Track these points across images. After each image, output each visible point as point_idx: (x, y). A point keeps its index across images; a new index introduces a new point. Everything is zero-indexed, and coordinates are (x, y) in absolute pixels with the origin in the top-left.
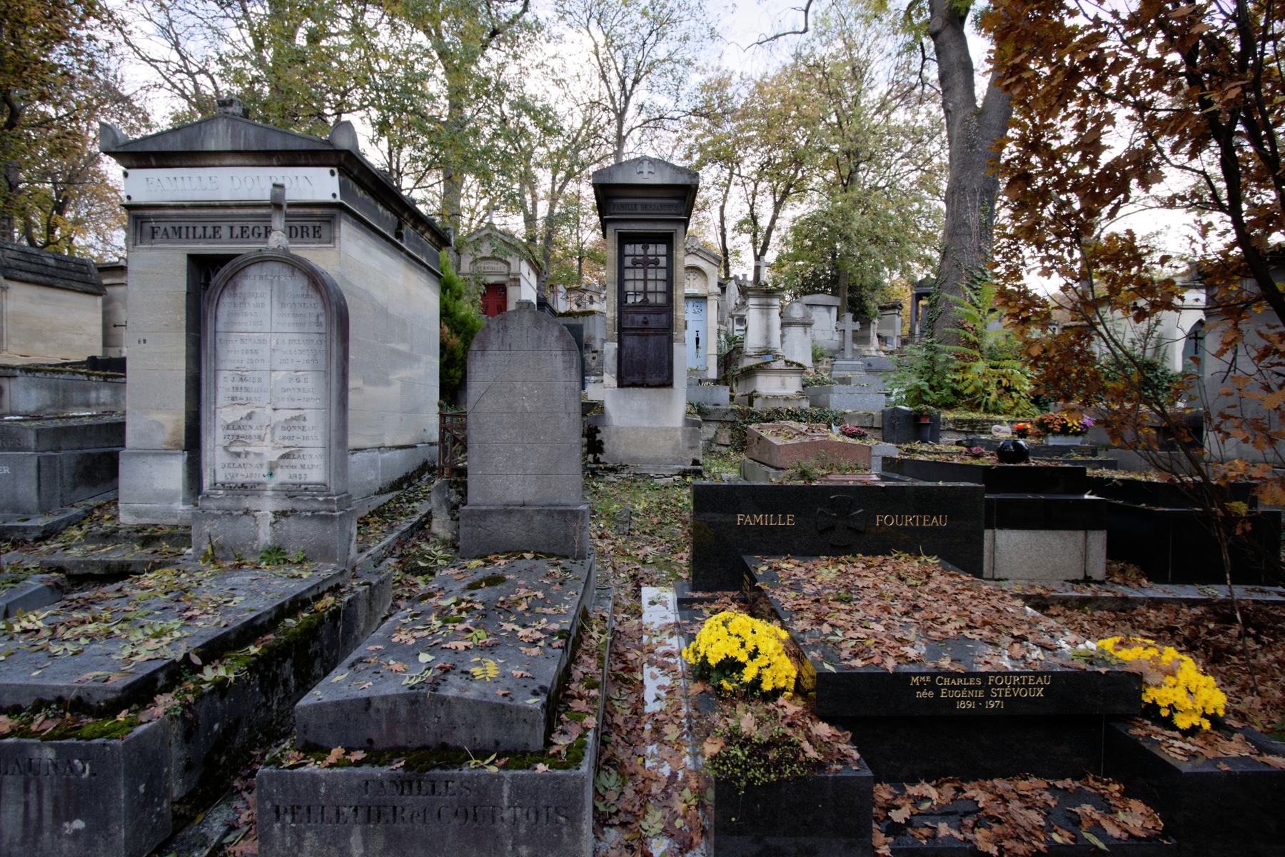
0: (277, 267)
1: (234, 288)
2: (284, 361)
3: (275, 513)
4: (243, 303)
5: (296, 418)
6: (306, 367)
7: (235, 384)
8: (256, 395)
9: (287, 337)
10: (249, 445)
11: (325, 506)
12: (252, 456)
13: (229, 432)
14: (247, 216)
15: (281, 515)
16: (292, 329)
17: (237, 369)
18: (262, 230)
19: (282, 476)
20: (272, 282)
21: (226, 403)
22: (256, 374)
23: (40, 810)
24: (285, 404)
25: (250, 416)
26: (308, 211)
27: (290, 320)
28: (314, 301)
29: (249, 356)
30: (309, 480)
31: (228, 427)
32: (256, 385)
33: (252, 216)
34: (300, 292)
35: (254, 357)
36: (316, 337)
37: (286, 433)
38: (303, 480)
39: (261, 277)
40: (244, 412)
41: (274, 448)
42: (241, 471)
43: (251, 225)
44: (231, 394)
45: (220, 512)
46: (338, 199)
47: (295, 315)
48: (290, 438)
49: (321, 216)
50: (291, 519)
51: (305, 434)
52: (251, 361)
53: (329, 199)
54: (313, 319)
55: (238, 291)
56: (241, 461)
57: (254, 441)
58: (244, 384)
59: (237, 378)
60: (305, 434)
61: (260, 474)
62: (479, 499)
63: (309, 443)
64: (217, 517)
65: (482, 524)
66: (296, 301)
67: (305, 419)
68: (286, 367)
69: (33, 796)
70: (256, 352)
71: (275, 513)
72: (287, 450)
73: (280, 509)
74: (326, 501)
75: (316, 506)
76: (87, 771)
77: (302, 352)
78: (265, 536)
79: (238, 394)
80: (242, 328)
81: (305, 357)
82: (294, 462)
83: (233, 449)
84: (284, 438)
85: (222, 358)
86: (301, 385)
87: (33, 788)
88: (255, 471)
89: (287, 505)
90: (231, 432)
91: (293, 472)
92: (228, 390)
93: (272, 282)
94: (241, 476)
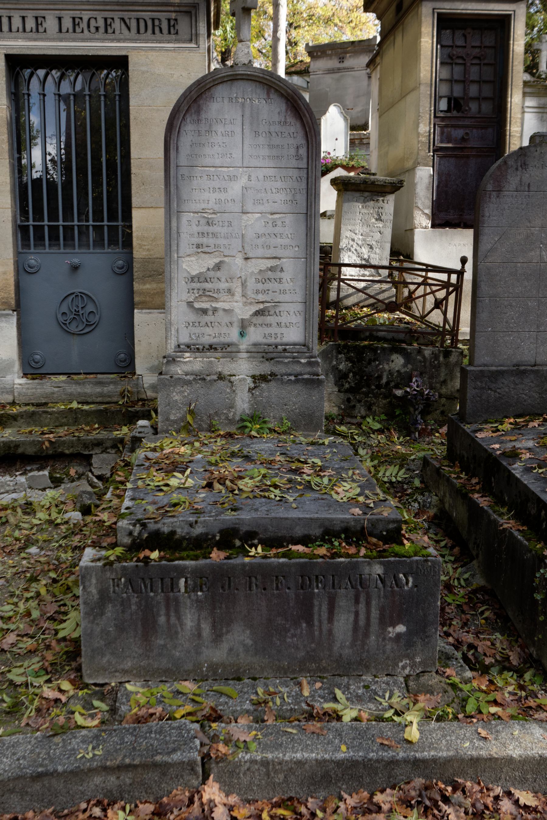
0: (249, 88)
1: (198, 112)
2: (259, 202)
3: (253, 377)
4: (209, 131)
5: (272, 269)
7: (200, 229)
8: (225, 242)
10: (216, 300)
11: (308, 369)
12: (221, 313)
13: (194, 285)
15: (260, 379)
17: (204, 211)
18: (101, 23)
19: (255, 335)
21: (189, 252)
23: (368, 618)
24: (260, 252)
25: (218, 267)
27: (265, 152)
28: (292, 129)
29: (217, 195)
30: (285, 340)
35: (222, 196)
37: (260, 286)
38: (278, 340)
39: (231, 99)
40: (211, 262)
41: (245, 304)
42: (208, 330)
43: (86, 16)
45: (190, 378)
48: (264, 292)
50: (272, 384)
51: (281, 287)
52: (219, 202)
54: (293, 151)
55: (203, 116)
57: (223, 296)
58: (211, 229)
59: (203, 221)
60: (281, 287)
61: (233, 335)
62: (487, 359)
63: (287, 297)
64: (188, 383)
65: (493, 386)
66: (272, 129)
67: (282, 270)
68: (261, 208)
69: (362, 607)
71: (253, 377)
72: (261, 306)
73: (258, 373)
74: (310, 364)
75: (298, 369)
76: (410, 584)
77: (278, 190)
78: (243, 403)
79: (205, 241)
80: (208, 161)
81: (281, 197)
82: (269, 319)
83: (197, 305)
84: (257, 292)
85: (185, 196)
86: (277, 230)
87: (362, 599)
88: (224, 330)
89: (266, 368)
91: (268, 331)
92: (192, 235)
93: (243, 105)
94: (208, 336)
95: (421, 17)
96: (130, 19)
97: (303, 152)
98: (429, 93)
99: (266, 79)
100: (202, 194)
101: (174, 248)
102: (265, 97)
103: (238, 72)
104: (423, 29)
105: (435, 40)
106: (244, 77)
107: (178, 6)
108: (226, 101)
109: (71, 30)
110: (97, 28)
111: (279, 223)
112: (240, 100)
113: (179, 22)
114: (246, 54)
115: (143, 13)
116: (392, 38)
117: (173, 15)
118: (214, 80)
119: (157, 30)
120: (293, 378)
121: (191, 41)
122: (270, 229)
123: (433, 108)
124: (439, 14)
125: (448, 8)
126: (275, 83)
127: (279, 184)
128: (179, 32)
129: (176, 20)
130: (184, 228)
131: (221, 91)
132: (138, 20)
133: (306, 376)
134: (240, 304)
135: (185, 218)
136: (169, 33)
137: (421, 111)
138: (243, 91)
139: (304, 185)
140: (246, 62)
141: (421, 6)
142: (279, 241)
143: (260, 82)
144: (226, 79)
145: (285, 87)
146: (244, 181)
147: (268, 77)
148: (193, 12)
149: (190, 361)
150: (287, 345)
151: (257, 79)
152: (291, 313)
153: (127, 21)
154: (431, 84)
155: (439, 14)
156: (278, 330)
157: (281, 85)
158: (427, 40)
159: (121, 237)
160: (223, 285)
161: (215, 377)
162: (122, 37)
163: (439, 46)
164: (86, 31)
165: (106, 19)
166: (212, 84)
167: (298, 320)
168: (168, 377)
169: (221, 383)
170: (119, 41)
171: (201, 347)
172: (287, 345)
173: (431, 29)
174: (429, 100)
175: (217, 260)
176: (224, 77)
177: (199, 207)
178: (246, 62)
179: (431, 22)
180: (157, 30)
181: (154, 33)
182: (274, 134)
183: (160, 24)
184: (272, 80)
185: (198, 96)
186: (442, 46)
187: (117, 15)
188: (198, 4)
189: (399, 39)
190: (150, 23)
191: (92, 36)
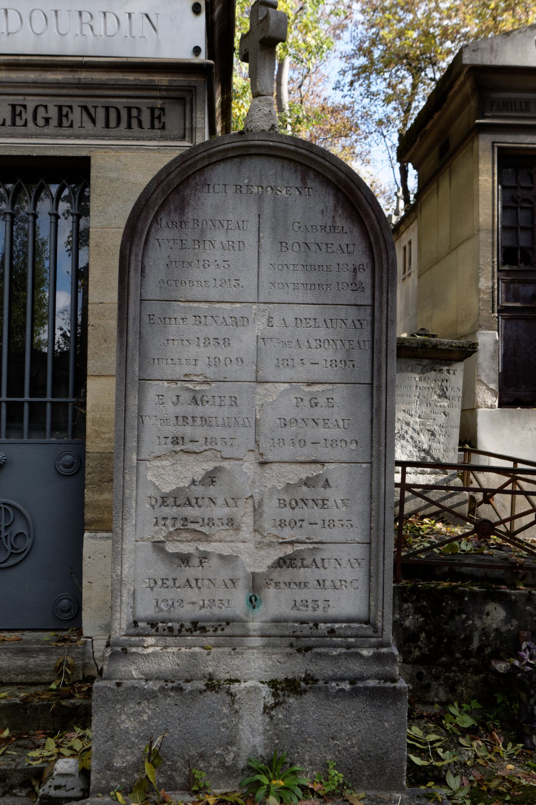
0: (269, 171)
1: (182, 208)
2: (286, 363)
3: (273, 684)
4: (200, 241)
5: (308, 482)
6: (331, 374)
7: (180, 410)
8: (225, 433)
9: (290, 313)
10: (206, 538)
11: (375, 669)
12: (214, 562)
13: (166, 511)
14: (26, 84)
15: (285, 688)
16: (302, 296)
17: (187, 378)
18: (53, 113)
19: (277, 603)
20: (260, 198)
21: (158, 450)
22: (227, 389)
24: (287, 452)
25: (211, 478)
26: (144, 78)
27: (299, 276)
28: (346, 239)
29: (212, 351)
30: (332, 612)
31: (164, 500)
32: (223, 413)
33: (35, 84)
34: (318, 220)
35: (221, 353)
36: (352, 314)
37: (287, 514)
38: (320, 613)
39: (238, 188)
40: (199, 468)
41: (259, 545)
42: (191, 594)
43: (31, 103)
44: (171, 430)
46: (202, 58)
47: (308, 268)
48: (295, 523)
49: (168, 88)
50: (309, 697)
51: (326, 514)
52: (215, 362)
53: (184, 54)
54: (346, 276)
55: (190, 215)
56: (191, 572)
57: (219, 531)
58: (199, 410)
59: (186, 397)
61: (237, 603)
63: (336, 534)
64: (151, 696)
66: (311, 238)
67: (327, 484)
68: (289, 374)
70: (227, 342)
71: (273, 684)
72: (289, 550)
73: (281, 676)
74: (378, 658)
75: (356, 668)
77: (320, 343)
78: (252, 735)
79: (188, 431)
80: (196, 292)
81: (327, 354)
82: (302, 574)
83: (171, 548)
84: (282, 524)
85: (154, 353)
86: (320, 412)
88: (220, 594)
89: (297, 667)
90: (170, 511)
91: (301, 595)
92: (165, 421)
93: (260, 198)
94: (191, 605)
95: (478, 152)
96: (96, 107)
97: (364, 277)
98: (490, 240)
99: (301, 154)
100: (185, 348)
101: (132, 443)
102: (299, 184)
103: (251, 143)
104: (481, 166)
105: (496, 178)
106: (263, 151)
107: (166, 90)
108: (230, 190)
109: (8, 122)
110: (47, 120)
111: (322, 401)
112: (255, 190)
113: (166, 112)
114: (265, 115)
115: (116, 100)
116: (434, 186)
117: (159, 103)
118: (210, 156)
119: (134, 122)
120: (346, 686)
121: (183, 138)
122: (306, 412)
123: (496, 259)
124: (499, 148)
125: (511, 141)
126: (315, 161)
127: (322, 333)
128: (168, 126)
129: (162, 109)
130: (151, 407)
131: (221, 174)
132: (107, 109)
133: (372, 683)
134: (251, 546)
135: (153, 390)
136: (153, 127)
137: (481, 263)
138: (261, 175)
139: (366, 335)
140: (267, 128)
141: (478, 139)
142: (322, 432)
143: (290, 160)
144: (231, 155)
145: (334, 168)
146: (259, 326)
147: (304, 151)
148: (188, 99)
149: (154, 654)
150: (335, 621)
151: (285, 155)
152: (344, 563)
153: (92, 111)
154: (493, 230)
155: (499, 148)
156: (319, 594)
157: (327, 164)
158: (487, 179)
159: (72, 421)
160: (220, 512)
161: (201, 685)
162: (83, 131)
163: (500, 187)
164: (30, 124)
165: (60, 108)
166: (206, 163)
167: (356, 575)
168: (111, 684)
169: (212, 696)
170: (78, 137)
171: (176, 626)
172: (335, 621)
173: (490, 166)
174: (491, 249)
175: (209, 466)
176: (228, 149)
177: (179, 371)
178: (267, 128)
179: (490, 158)
180: (134, 122)
181: (129, 127)
182: (313, 247)
183: (140, 116)
184: (312, 155)
185: (182, 183)
186: (504, 187)
187: (76, 103)
188: (195, 87)
189: (444, 184)
190: (124, 114)
191: (39, 130)
